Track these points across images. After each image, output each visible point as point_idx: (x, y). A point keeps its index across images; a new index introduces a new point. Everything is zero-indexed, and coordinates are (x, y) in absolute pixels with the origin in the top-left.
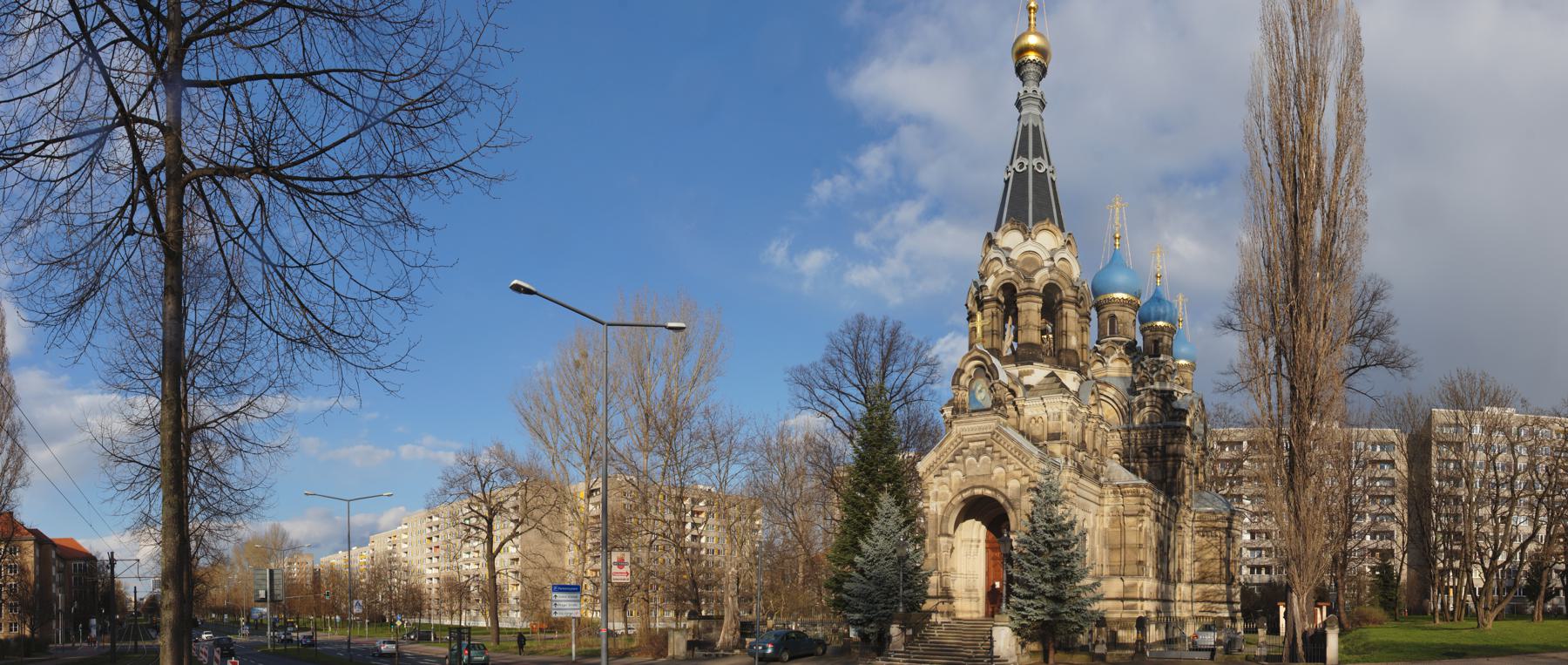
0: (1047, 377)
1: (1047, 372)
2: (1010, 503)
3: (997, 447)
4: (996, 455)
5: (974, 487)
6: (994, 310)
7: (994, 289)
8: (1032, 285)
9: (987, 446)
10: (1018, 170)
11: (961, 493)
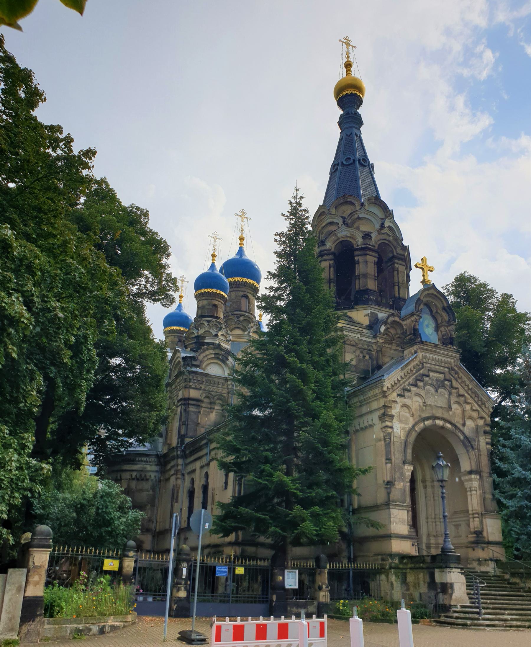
3: (455, 384)
9: (446, 380)
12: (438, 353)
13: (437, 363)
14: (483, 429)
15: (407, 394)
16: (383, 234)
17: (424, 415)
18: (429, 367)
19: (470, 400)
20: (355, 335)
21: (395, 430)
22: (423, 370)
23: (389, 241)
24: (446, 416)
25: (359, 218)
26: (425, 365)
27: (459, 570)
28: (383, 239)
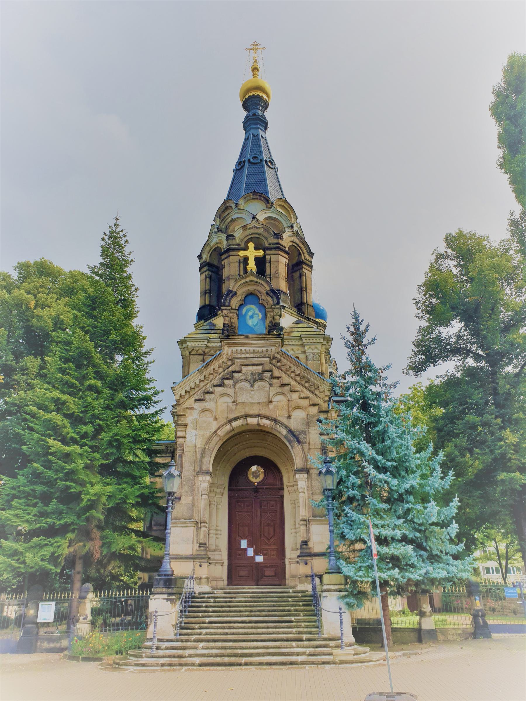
1: (295, 320)
2: (294, 435)
3: (277, 373)
5: (246, 416)
8: (281, 242)
9: (264, 371)
11: (230, 422)
12: (252, 344)
13: (252, 355)
14: (316, 418)
15: (208, 396)
16: (250, 228)
17: (232, 416)
18: (240, 362)
19: (299, 388)
20: (202, 343)
21: (188, 439)
22: (233, 366)
23: (259, 234)
24: (264, 411)
25: (233, 220)
26: (236, 360)
27: (165, 596)
28: (251, 234)
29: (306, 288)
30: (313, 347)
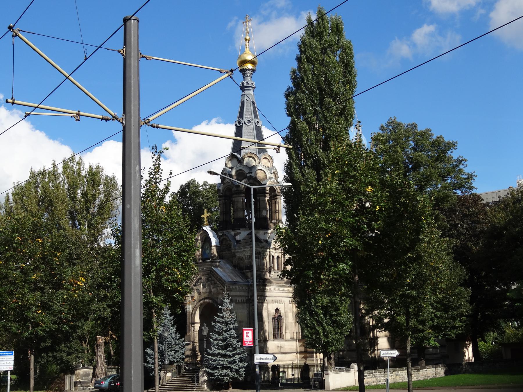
0: (248, 235)
4: (213, 282)
6: (224, 201)
7: (223, 190)
10: (238, 125)
11: (199, 301)
17: (201, 298)
19: (220, 285)
23: (230, 185)
29: (259, 209)
30: (247, 252)
